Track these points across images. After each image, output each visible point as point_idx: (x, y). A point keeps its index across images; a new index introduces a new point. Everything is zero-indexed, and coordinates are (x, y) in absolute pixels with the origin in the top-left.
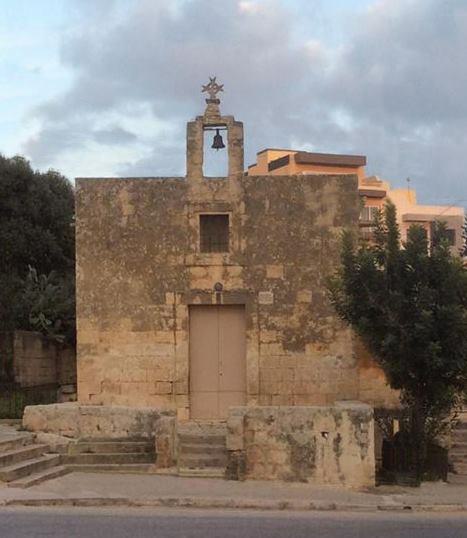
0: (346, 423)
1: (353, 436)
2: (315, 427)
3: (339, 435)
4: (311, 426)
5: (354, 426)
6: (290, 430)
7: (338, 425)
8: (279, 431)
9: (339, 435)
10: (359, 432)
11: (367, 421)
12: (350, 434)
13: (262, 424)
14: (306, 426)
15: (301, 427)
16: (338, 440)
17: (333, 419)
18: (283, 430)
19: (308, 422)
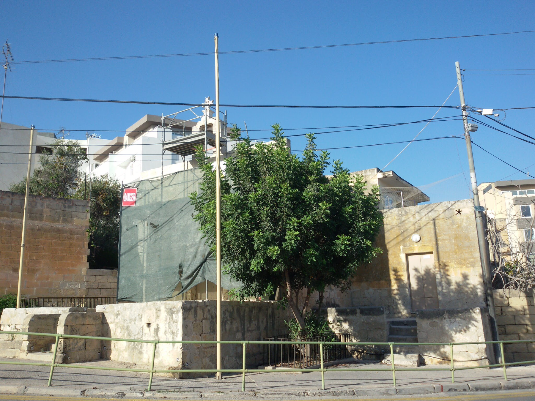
0: (163, 314)
1: (167, 326)
2: (143, 318)
3: (158, 325)
4: (141, 317)
5: (168, 317)
6: (129, 321)
7: (158, 317)
8: (122, 323)
9: (158, 325)
10: (172, 323)
11: (178, 311)
12: (166, 324)
13: (113, 317)
14: (138, 318)
15: (135, 320)
16: (157, 329)
17: (155, 311)
18: (125, 321)
19: (139, 315)
